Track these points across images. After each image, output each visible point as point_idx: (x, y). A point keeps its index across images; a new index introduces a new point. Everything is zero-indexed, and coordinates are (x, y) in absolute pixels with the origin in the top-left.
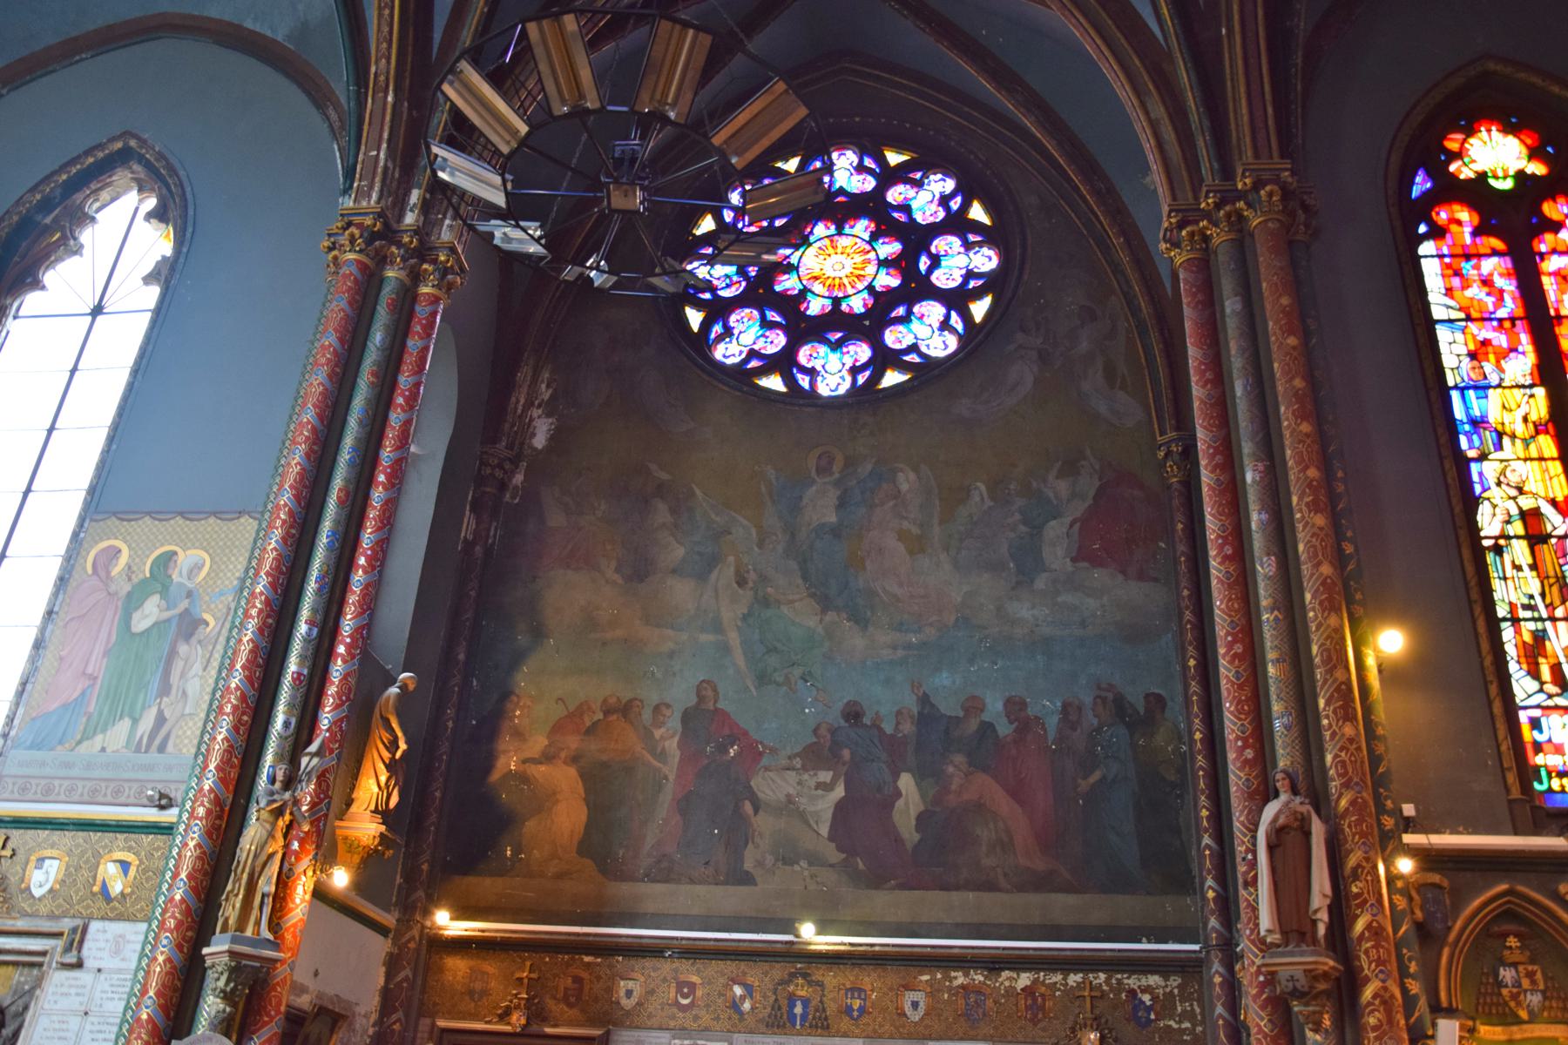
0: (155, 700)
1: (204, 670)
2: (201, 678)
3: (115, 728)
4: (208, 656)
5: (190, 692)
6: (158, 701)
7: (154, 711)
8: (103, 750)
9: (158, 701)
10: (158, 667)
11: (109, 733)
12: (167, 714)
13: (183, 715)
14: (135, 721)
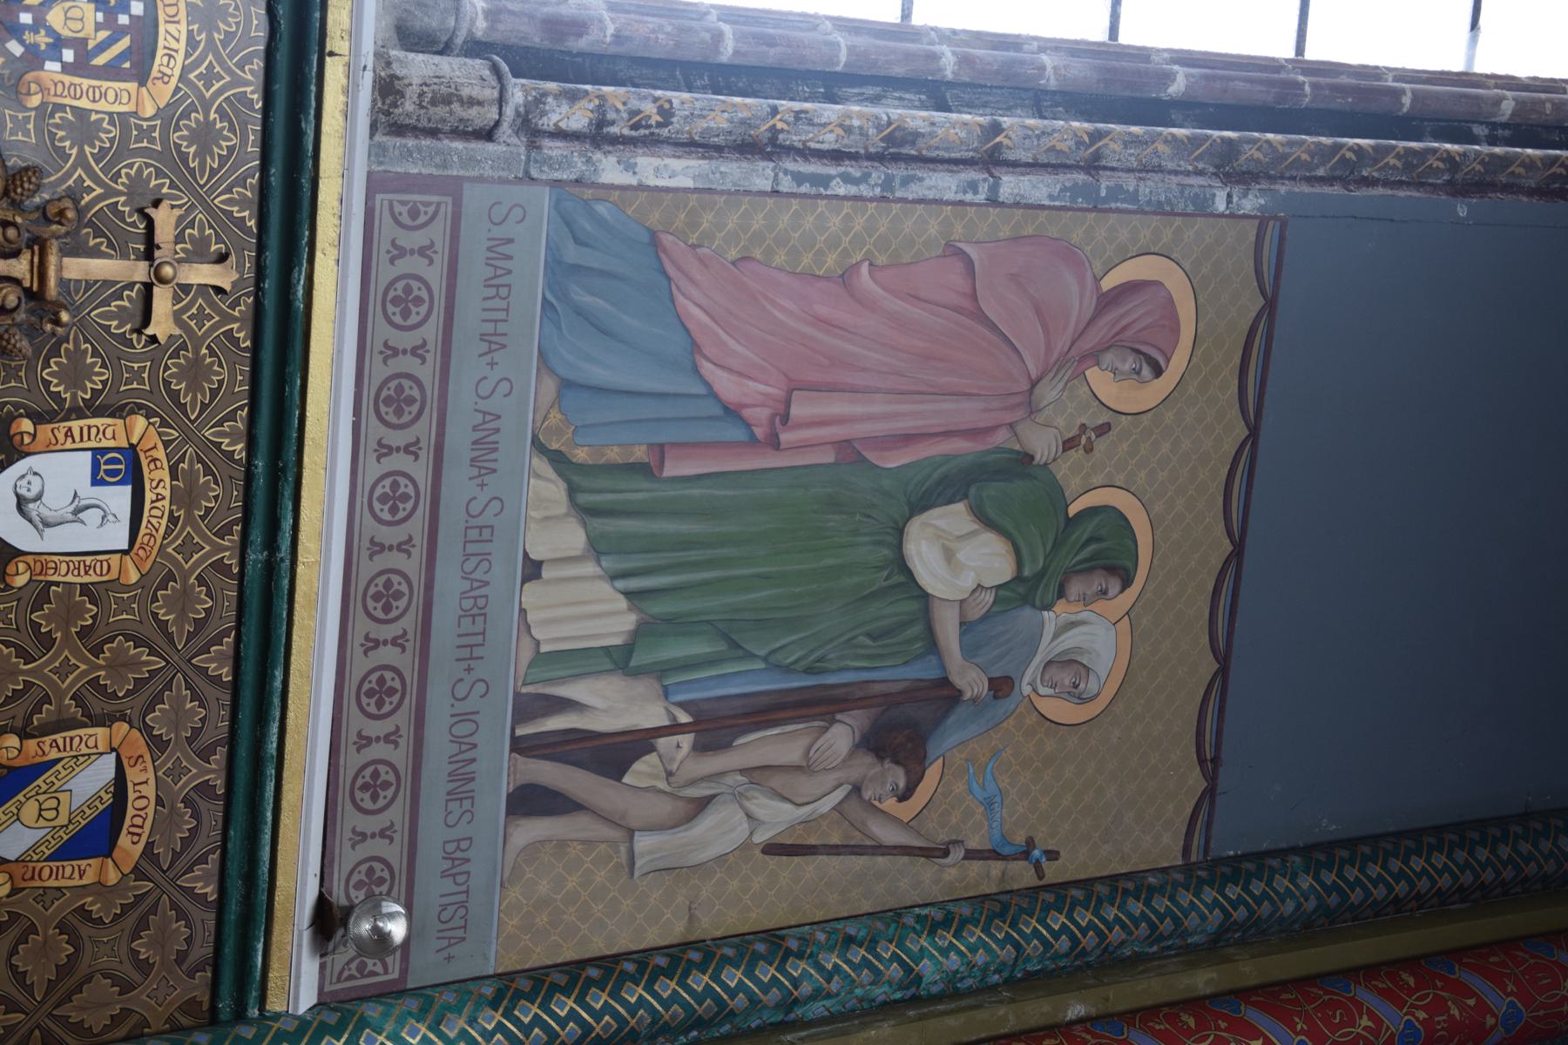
0: (683, 705)
1: (772, 849)
2: (746, 847)
3: (605, 588)
4: (812, 841)
5: (707, 823)
6: (684, 718)
7: (652, 715)
8: (533, 570)
9: (684, 718)
10: (788, 669)
11: (590, 568)
12: (643, 771)
13: (631, 832)
14: (620, 660)
